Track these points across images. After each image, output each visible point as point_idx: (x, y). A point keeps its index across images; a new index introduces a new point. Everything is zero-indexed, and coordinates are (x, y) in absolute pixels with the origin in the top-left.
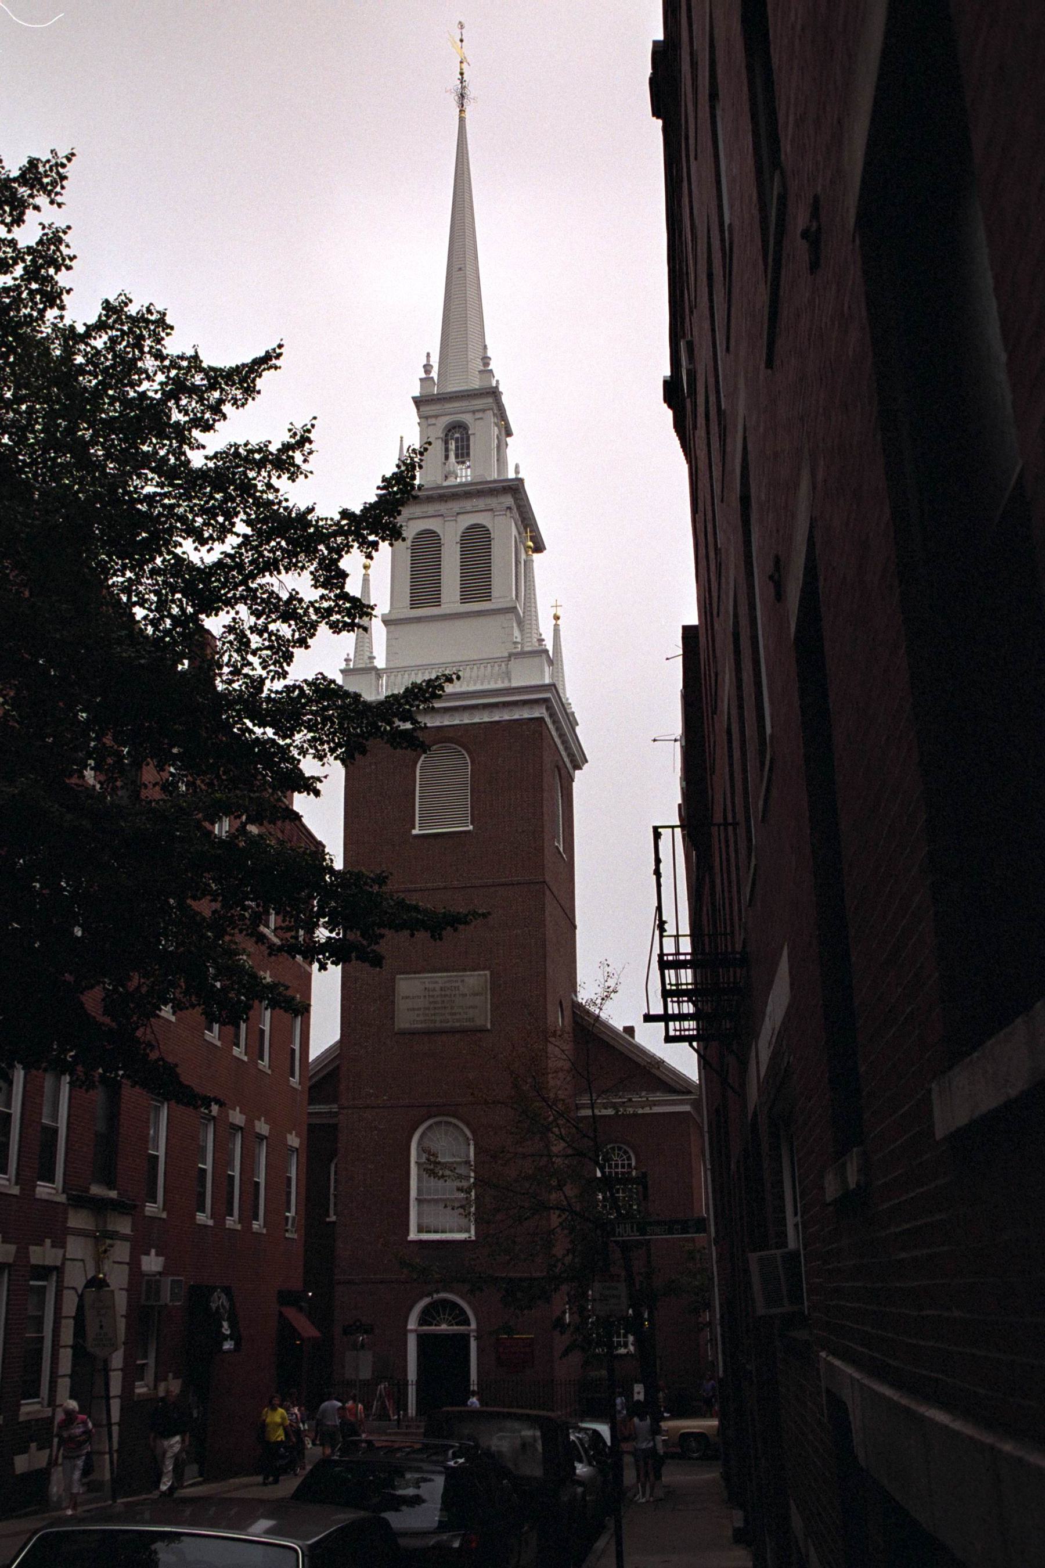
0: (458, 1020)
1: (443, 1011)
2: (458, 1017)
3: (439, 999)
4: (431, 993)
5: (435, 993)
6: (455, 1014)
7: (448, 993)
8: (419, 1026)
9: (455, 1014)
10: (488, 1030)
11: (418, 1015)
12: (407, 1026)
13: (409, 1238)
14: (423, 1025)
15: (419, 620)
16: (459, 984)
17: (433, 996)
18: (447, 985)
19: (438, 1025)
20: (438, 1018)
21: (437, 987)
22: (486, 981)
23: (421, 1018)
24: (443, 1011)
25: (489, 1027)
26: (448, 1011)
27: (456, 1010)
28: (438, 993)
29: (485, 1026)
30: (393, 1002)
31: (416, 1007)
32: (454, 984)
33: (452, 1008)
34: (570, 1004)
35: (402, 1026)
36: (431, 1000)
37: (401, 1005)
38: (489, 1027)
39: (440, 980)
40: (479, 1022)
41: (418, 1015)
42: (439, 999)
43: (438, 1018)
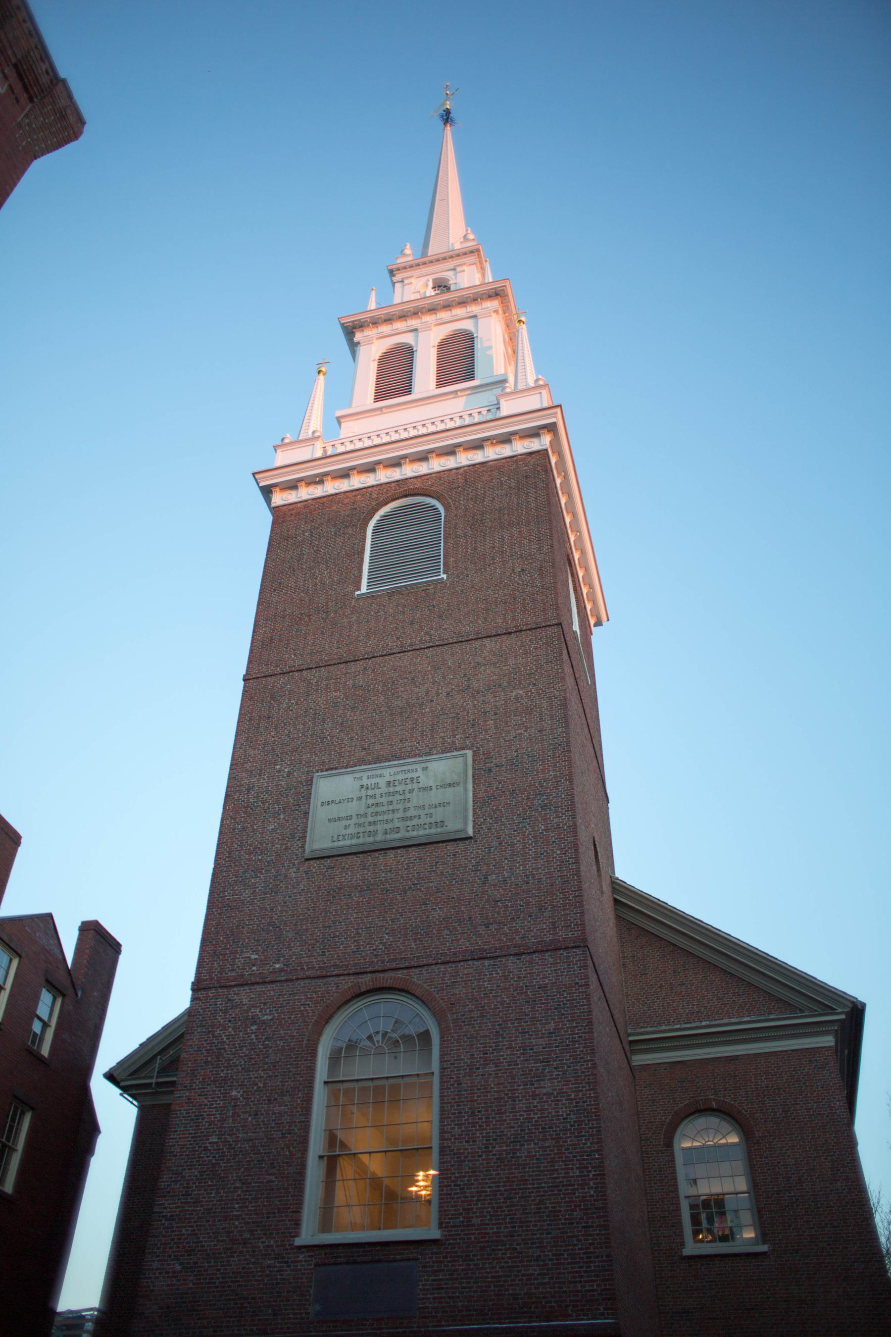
0: (419, 826)
1: (390, 816)
4: (370, 792)
5: (378, 792)
6: (411, 818)
7: (399, 788)
8: (348, 842)
9: (411, 818)
10: (471, 838)
11: (346, 827)
12: (327, 844)
13: (298, 1242)
14: (354, 841)
15: (381, 409)
18: (400, 777)
19: (380, 837)
20: (380, 828)
21: (382, 782)
22: (466, 764)
23: (352, 830)
24: (390, 816)
25: (470, 832)
26: (400, 814)
27: (412, 812)
28: (384, 789)
30: (306, 813)
31: (343, 815)
32: (414, 775)
33: (405, 810)
34: (608, 882)
35: (316, 846)
36: (370, 801)
37: (319, 815)
38: (470, 832)
39: (386, 772)
40: (453, 826)
41: (346, 827)
42: (384, 800)
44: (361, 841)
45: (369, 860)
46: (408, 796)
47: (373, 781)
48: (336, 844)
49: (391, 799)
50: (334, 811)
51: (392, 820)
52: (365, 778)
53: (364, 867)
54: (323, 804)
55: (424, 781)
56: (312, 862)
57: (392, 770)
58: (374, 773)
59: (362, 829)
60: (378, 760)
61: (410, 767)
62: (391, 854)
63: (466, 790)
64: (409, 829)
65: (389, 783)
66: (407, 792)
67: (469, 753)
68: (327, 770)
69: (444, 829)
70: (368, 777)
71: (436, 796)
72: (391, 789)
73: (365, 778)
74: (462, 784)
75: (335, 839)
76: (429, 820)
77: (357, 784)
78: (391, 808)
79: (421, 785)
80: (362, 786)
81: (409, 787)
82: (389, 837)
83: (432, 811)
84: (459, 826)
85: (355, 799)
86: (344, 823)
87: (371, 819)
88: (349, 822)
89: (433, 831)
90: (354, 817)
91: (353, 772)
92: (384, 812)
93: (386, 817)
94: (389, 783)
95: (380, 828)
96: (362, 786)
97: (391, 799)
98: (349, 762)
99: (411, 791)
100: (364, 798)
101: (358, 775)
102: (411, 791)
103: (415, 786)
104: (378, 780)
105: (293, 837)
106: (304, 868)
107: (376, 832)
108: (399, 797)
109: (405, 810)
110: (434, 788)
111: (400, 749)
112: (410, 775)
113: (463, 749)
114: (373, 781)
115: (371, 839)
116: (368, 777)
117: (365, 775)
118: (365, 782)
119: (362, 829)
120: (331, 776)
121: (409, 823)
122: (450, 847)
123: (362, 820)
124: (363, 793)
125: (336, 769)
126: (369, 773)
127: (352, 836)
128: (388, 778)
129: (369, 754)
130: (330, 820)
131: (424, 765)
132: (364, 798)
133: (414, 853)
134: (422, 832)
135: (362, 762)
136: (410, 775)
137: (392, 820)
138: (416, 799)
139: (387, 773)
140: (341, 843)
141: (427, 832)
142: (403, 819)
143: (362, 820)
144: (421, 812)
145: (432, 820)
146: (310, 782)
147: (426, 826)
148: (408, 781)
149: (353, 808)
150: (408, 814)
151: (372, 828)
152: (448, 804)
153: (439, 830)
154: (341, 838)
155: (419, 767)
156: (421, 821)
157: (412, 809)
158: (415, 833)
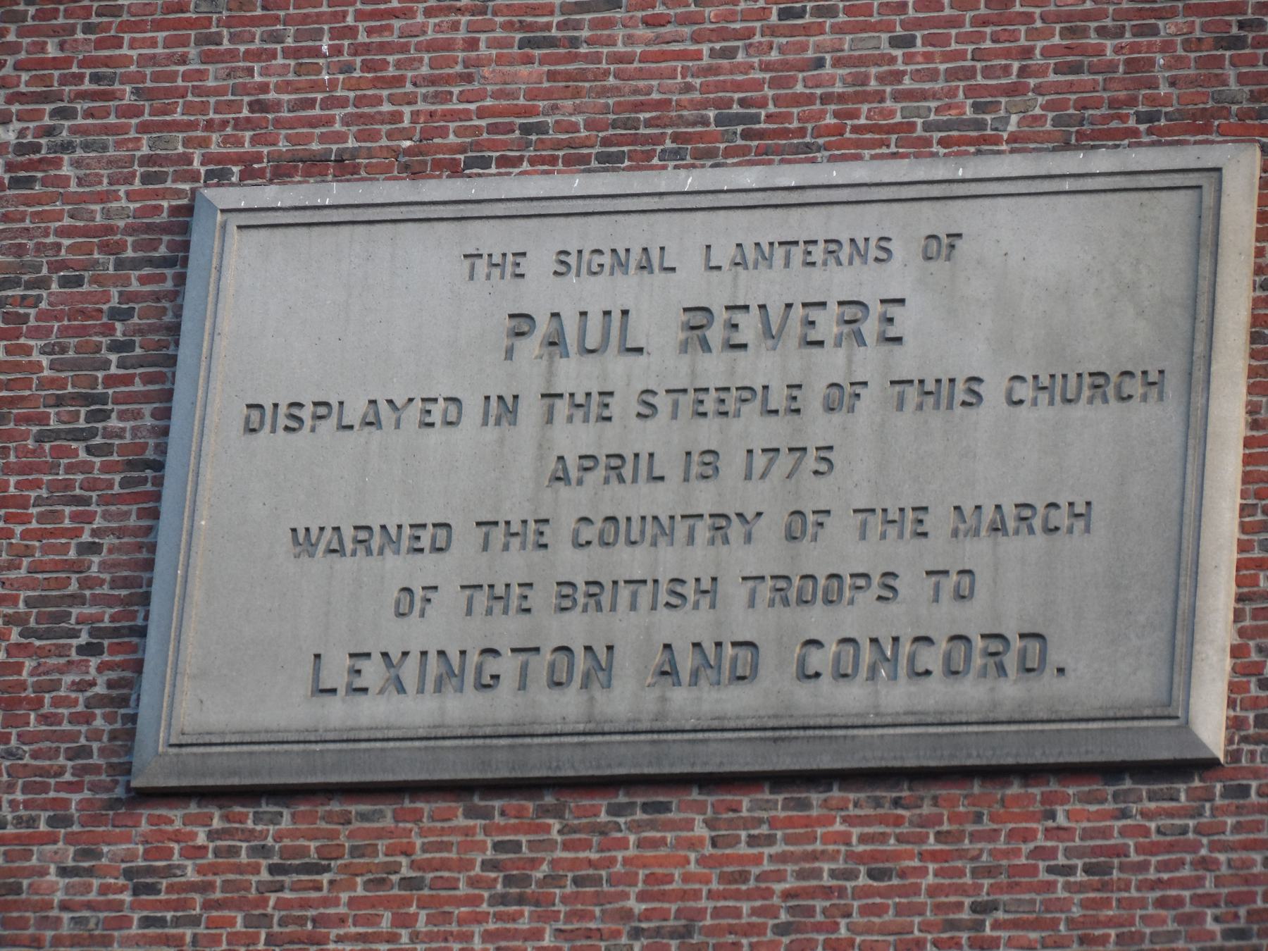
0: (885, 655)
2: (859, 617)
3: (663, 438)
4: (574, 375)
5: (622, 374)
6: (833, 590)
7: (763, 367)
8: (417, 710)
9: (833, 590)
11: (408, 602)
14: (460, 708)
16: (898, 277)
17: (596, 406)
18: (773, 286)
19: (625, 699)
21: (655, 308)
23: (441, 628)
25: (1211, 727)
26: (765, 553)
28: (665, 364)
29: (1171, 710)
30: (146, 471)
31: (389, 512)
32: (867, 283)
33: (798, 526)
36: (575, 438)
38: (1211, 727)
39: (682, 238)
40: (1096, 676)
41: (408, 602)
42: (663, 438)
43: (633, 631)
44: (502, 707)
45: (552, 838)
46: (819, 428)
47: (597, 294)
48: (337, 713)
49: (707, 434)
50: (339, 478)
51: (709, 591)
52: (540, 263)
53: (516, 888)
54: (256, 418)
55: (939, 338)
56: (176, 816)
57: (729, 232)
58: (596, 233)
59: (508, 630)
60: (624, 144)
61: (842, 224)
62: (695, 818)
63: (1195, 430)
64: (816, 660)
65: (697, 322)
66: (813, 400)
67: (1241, 167)
68: (282, 172)
69: (1045, 689)
70: (563, 265)
71: (1001, 456)
72: (714, 368)
73: (540, 263)
74: (1173, 384)
75: (335, 675)
76: (944, 619)
77: (492, 301)
78: (705, 498)
79: (906, 363)
80: (521, 324)
81: (832, 364)
82: (685, 702)
83: (977, 552)
84: (1137, 682)
85: (473, 409)
86: (398, 569)
87: (575, 565)
88: (426, 569)
89: (971, 693)
90: (466, 538)
91: (462, 213)
92: (661, 529)
93: (667, 561)
94: (697, 322)
95: (633, 631)
96: (521, 324)
97: (707, 434)
98: (431, 128)
99: (842, 397)
100: (531, 409)
101: (492, 238)
102: (842, 397)
103: (869, 362)
104: (623, 290)
105: (55, 626)
106: (126, 846)
107: (601, 666)
108: (754, 429)
109: (798, 526)
110: (993, 391)
111: (781, 74)
112: (840, 282)
113: (1199, 123)
114: (597, 294)
115: (566, 706)
116: (563, 265)
117: (542, 243)
118: (541, 293)
119: (508, 630)
120: (312, 220)
121: (816, 621)
122: (1074, 808)
123: (514, 565)
124: (528, 371)
125: (345, 167)
126: (573, 235)
127: (449, 672)
128: (692, 285)
129: (569, 84)
130: (303, 541)
131: (934, 219)
132: (531, 409)
133: (843, 822)
134: (898, 696)
135: (517, 140)
136: (840, 282)
137: (709, 591)
138: (873, 455)
139: (687, 247)
140: (374, 711)
141: (936, 694)
142: (788, 590)
143: (514, 565)
144: (902, 555)
145: (972, 619)
146: (171, 245)
147: (931, 658)
148: (827, 325)
149: (452, 473)
150: (817, 558)
151: (575, 628)
152: (1082, 514)
153: (1012, 691)
154: (373, 672)
155: (908, 226)
156: (897, 620)
157: (841, 528)
158: (850, 698)
